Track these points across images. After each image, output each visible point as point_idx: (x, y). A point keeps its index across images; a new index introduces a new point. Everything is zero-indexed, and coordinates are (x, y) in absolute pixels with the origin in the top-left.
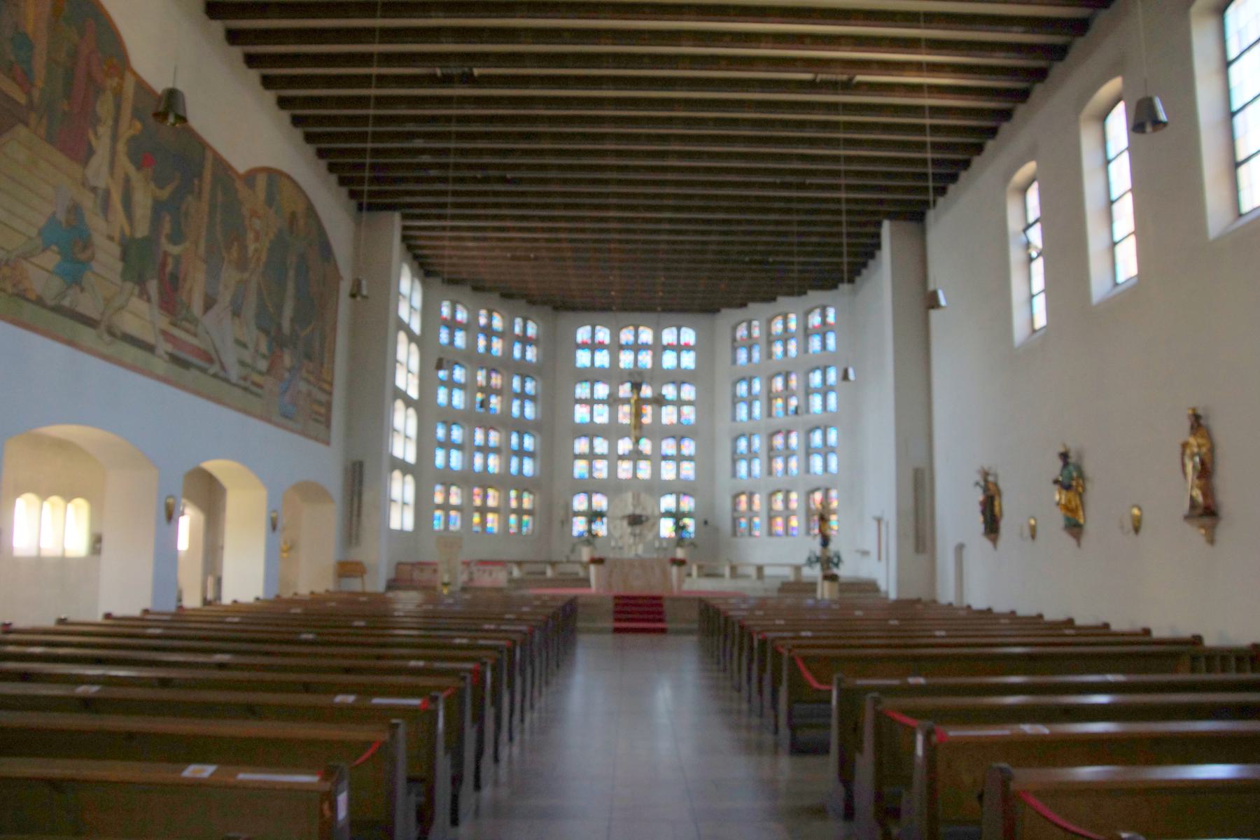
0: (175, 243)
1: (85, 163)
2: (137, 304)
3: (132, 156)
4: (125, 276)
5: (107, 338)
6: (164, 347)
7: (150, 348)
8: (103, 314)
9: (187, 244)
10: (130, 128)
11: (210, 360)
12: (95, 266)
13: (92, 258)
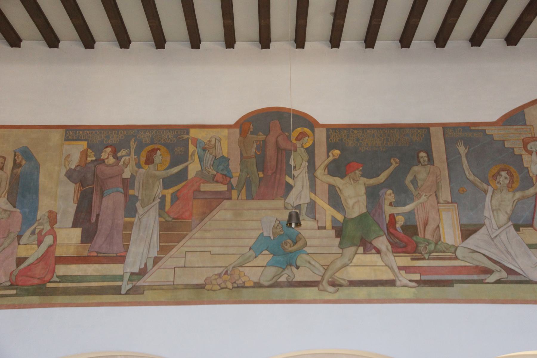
0: (405, 205)
1: (286, 195)
2: (361, 258)
3: (332, 173)
4: (341, 246)
5: (331, 289)
6: (404, 278)
7: (391, 283)
8: (323, 276)
9: (423, 198)
10: (322, 158)
11: (488, 272)
12: (307, 250)
13: (305, 245)
